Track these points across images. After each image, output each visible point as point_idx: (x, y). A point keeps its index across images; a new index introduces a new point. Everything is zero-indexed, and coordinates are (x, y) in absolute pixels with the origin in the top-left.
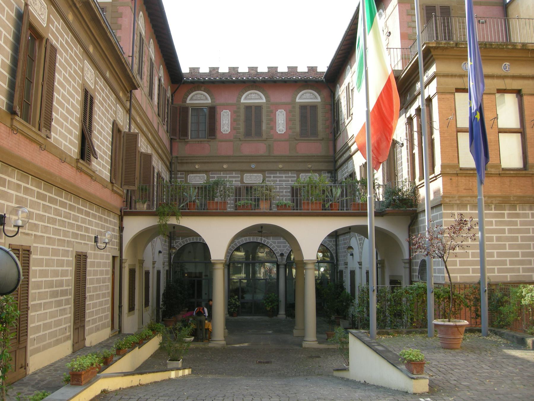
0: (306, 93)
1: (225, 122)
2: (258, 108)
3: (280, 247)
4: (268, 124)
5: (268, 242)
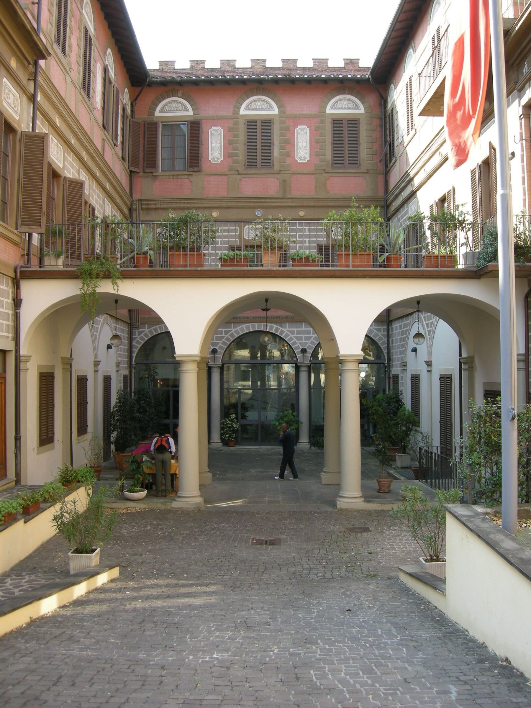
0: (341, 100)
1: (215, 146)
2: (267, 123)
3: (300, 338)
4: (282, 148)
5: (282, 332)
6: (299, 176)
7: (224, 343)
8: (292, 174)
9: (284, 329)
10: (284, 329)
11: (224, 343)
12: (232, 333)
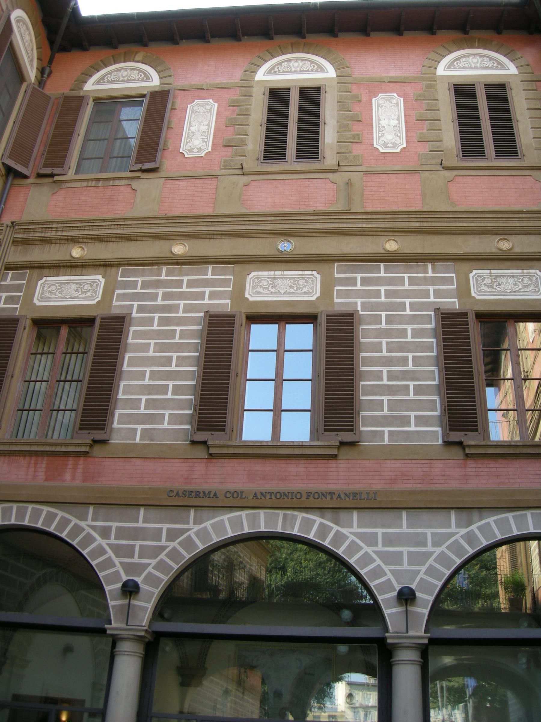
1: (197, 129)
2: (311, 96)
3: (396, 559)
4: (342, 128)
5: (339, 538)
6: (384, 177)
7: (161, 566)
8: (367, 173)
9: (345, 531)
10: (345, 531)
11: (161, 566)
12: (189, 538)
